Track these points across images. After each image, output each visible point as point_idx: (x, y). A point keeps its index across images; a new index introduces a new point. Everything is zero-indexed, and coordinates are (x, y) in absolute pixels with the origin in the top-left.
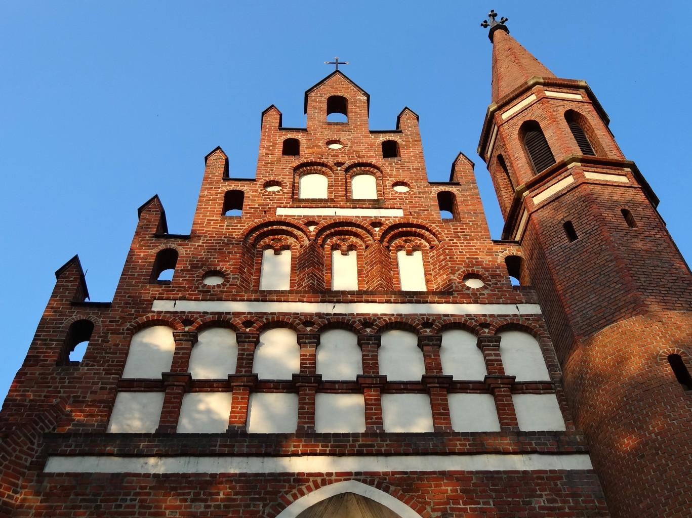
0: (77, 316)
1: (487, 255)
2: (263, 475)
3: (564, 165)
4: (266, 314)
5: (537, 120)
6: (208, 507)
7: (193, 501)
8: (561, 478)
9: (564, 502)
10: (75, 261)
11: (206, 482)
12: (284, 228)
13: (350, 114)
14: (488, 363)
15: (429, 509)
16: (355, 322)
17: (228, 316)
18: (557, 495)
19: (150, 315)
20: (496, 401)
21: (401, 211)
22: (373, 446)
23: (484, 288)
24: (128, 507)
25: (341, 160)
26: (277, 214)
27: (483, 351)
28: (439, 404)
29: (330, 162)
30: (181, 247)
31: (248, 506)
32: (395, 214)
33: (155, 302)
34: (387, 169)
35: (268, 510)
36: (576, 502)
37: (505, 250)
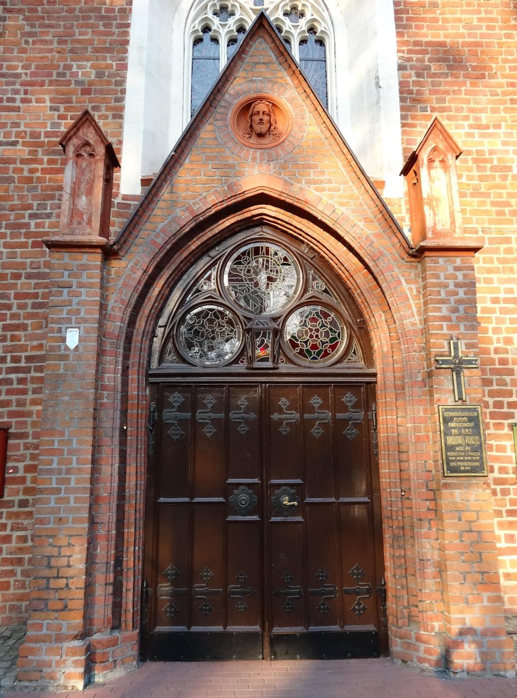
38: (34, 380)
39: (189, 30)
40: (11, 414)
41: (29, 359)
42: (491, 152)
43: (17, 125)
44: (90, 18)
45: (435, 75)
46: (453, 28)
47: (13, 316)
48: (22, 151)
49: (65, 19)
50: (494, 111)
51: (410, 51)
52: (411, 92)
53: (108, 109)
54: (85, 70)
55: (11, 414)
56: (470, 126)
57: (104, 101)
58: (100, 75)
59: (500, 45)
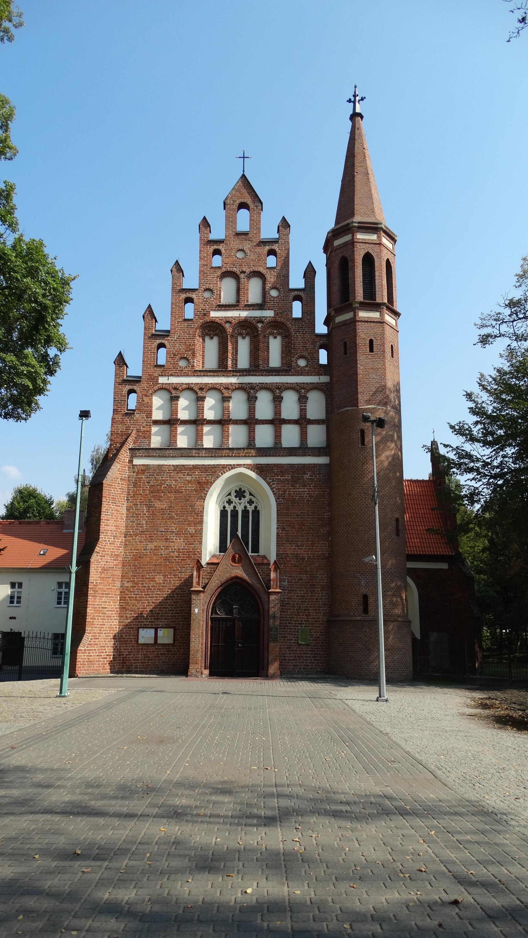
1: (311, 344)
2: (210, 465)
4: (208, 384)
6: (192, 478)
9: (315, 476)
11: (191, 468)
13: (251, 211)
14: (301, 410)
15: (268, 479)
16: (247, 388)
17: (193, 385)
18: (314, 474)
20: (301, 427)
21: (273, 311)
23: (306, 366)
24: (165, 477)
25: (244, 269)
26: (211, 316)
27: (301, 403)
28: (278, 432)
31: (206, 477)
32: (269, 314)
34: (268, 276)
37: (320, 340)
38: (181, 616)
41: (180, 610)
42: (300, 554)
43: (174, 546)
44: (192, 513)
46: (293, 516)
47: (176, 599)
48: (176, 554)
50: (302, 541)
51: (280, 523)
52: (279, 536)
53: (198, 541)
54: (191, 530)
56: (295, 546)
57: (197, 539)
58: (196, 531)
59: (306, 521)
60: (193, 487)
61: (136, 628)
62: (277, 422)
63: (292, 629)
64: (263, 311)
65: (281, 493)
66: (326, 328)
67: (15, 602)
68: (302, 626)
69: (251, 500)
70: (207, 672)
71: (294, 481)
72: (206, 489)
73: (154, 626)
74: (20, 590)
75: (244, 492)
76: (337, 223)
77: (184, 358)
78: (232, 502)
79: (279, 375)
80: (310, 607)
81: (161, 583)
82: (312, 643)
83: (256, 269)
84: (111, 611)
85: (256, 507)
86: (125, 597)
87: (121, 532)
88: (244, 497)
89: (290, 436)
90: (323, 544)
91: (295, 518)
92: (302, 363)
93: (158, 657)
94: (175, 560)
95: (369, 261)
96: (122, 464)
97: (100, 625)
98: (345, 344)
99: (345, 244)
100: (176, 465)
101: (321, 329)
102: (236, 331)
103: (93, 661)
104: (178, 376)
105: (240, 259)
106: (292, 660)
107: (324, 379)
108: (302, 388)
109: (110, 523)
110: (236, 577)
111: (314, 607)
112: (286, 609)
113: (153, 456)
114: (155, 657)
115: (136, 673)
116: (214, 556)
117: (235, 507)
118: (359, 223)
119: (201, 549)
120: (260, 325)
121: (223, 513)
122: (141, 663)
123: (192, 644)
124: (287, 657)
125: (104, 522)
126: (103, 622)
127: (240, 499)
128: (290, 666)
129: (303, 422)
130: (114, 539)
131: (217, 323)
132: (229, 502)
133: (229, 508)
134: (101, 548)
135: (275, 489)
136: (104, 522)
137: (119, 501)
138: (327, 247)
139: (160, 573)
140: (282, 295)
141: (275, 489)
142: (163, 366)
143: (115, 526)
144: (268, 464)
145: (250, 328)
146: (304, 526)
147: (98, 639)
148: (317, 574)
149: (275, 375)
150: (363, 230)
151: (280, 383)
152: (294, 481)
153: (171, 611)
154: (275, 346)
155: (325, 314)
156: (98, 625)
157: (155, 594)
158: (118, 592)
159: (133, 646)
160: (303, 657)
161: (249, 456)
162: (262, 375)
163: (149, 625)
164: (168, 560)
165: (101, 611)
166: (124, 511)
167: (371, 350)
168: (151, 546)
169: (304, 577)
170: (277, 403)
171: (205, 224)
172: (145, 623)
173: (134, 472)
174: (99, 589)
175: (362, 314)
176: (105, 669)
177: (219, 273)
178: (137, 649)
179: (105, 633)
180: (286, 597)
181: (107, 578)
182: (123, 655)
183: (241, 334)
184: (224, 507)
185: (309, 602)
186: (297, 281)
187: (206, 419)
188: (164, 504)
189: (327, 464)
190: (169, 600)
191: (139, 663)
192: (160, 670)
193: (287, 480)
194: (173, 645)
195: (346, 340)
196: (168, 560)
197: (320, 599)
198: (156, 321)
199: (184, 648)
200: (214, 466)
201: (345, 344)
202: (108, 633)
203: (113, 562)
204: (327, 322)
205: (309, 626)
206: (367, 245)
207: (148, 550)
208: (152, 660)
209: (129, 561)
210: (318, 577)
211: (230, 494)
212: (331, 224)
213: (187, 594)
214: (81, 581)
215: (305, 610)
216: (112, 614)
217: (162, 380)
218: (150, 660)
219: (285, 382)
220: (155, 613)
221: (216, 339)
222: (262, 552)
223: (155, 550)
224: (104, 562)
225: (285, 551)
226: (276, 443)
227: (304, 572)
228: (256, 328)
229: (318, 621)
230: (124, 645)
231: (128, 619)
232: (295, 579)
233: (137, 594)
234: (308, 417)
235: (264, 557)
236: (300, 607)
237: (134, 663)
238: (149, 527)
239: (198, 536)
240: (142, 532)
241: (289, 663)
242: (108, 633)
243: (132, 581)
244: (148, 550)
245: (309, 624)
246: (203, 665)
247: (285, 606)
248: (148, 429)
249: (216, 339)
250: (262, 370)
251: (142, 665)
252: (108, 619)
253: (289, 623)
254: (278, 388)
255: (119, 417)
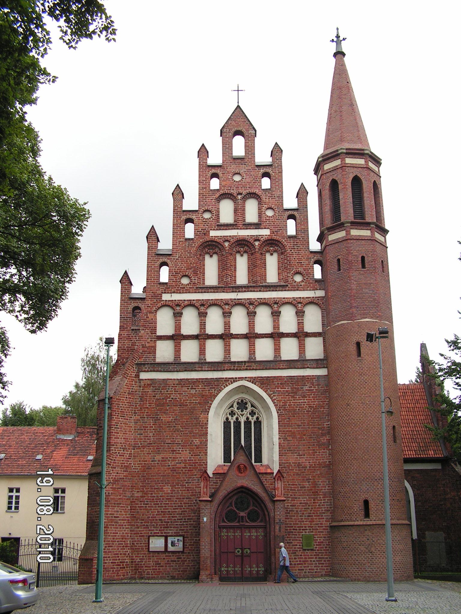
0: (134, 305)
3: (343, 224)
5: (338, 181)
7: (191, 389)
8: (315, 378)
10: (126, 271)
12: (214, 243)
15: (269, 391)
17: (194, 302)
18: (313, 385)
19: (162, 302)
22: (251, 366)
23: (302, 281)
25: (241, 191)
26: (211, 235)
29: (234, 192)
30: (169, 261)
31: (209, 390)
32: (265, 232)
33: (163, 295)
35: (216, 392)
36: (318, 387)
39: (223, 421)
40: (185, 532)
41: (188, 519)
45: (288, 441)
47: (184, 509)
49: (191, 426)
54: (197, 441)
55: (185, 532)
57: (202, 450)
60: (197, 400)
61: (146, 536)
62: (276, 336)
63: (296, 535)
64: (260, 230)
65: (281, 404)
66: (319, 244)
67: (13, 508)
68: (305, 532)
69: (252, 411)
70: (216, 578)
71: (294, 392)
72: (210, 402)
73: (164, 534)
74: (18, 494)
75: (246, 403)
76: (326, 148)
77: (186, 276)
78: (235, 414)
79: (276, 291)
80: (313, 513)
81: (169, 493)
82: (316, 548)
83: (252, 191)
84: (123, 520)
85: (257, 418)
86: (135, 507)
87: (129, 444)
88: (246, 408)
89: (289, 349)
90: (324, 452)
91: (296, 428)
92: (298, 278)
93: (168, 564)
94: (182, 470)
95: (357, 182)
96: (129, 379)
97: (113, 533)
98: (339, 260)
99: (335, 169)
100: (181, 379)
101: (315, 246)
102: (234, 249)
103: (108, 568)
104: (180, 293)
105: (237, 182)
106: (298, 564)
107: (320, 293)
108: (298, 303)
109: (120, 436)
110: (242, 487)
111: (317, 513)
112: (290, 516)
113: (157, 371)
114: (166, 564)
115: (148, 579)
116: (219, 466)
117: (237, 419)
118: (346, 149)
119: (207, 460)
120: (257, 243)
121: (227, 424)
122: (153, 569)
123: (202, 551)
124: (293, 562)
125: (114, 435)
126: (115, 531)
127: (242, 411)
128: (295, 570)
129: (301, 335)
130: (124, 451)
131: (216, 242)
132: (232, 414)
133: (232, 420)
134: (112, 460)
135: (275, 401)
136: (114, 435)
137: (127, 415)
138: (317, 170)
139: (168, 483)
140: (277, 214)
141: (275, 401)
142: (166, 283)
143: (124, 438)
144: (268, 377)
145: (248, 246)
146: (305, 435)
147: (112, 546)
148: (318, 482)
149: (273, 291)
150: (351, 156)
151: (277, 298)
152: (294, 392)
153: (180, 519)
154: (272, 262)
155: (318, 233)
156: (111, 533)
157: (164, 504)
158: (129, 502)
159: (145, 554)
160: (308, 561)
161: (250, 370)
162: (260, 291)
163: (159, 533)
164: (175, 470)
165: (114, 520)
166: (132, 424)
167: (363, 266)
168: (158, 457)
169: (307, 484)
170: (276, 317)
171: (203, 152)
172: (155, 531)
173: (140, 387)
174: (111, 499)
175: (355, 232)
176: (119, 576)
177: (217, 195)
178: (149, 556)
179: (118, 542)
180: (290, 504)
181: (118, 488)
182: (135, 562)
183: (239, 252)
184: (227, 419)
185: (312, 508)
186: (290, 201)
187: (208, 334)
188: (170, 417)
189: (325, 375)
190: (177, 509)
191: (150, 569)
192: (171, 576)
193: (287, 391)
194: (182, 552)
195: (339, 257)
196: (175, 470)
197: (322, 505)
198: (158, 241)
199: (193, 555)
200: (218, 380)
201: (339, 260)
202: (121, 541)
203: (123, 474)
204: (320, 239)
205: (313, 532)
206: (355, 169)
207: (156, 461)
208: (163, 566)
209: (138, 471)
210: (320, 484)
211: (232, 406)
212: (319, 150)
213: (194, 503)
214: (94, 491)
215: (309, 516)
216: (124, 523)
217: (166, 297)
218: (162, 566)
219: (283, 297)
220: (165, 522)
221: (215, 257)
222: (265, 461)
223: (162, 461)
224: (115, 473)
225: (288, 460)
226: (275, 356)
227: (307, 480)
228: (253, 246)
229: (322, 527)
230: (136, 553)
231: (138, 528)
232: (298, 487)
233: (147, 504)
234: (305, 331)
235: (268, 466)
236: (303, 514)
237: (146, 570)
238: (157, 439)
239: (203, 448)
240: (149, 444)
241: (295, 567)
242: (121, 541)
243: (141, 491)
244: (156, 461)
245: (313, 529)
246: (213, 571)
247: (289, 513)
248: (153, 345)
249: (215, 257)
250: (260, 286)
251: (154, 572)
252: (120, 528)
253: (293, 529)
254: (276, 303)
255: (125, 333)
